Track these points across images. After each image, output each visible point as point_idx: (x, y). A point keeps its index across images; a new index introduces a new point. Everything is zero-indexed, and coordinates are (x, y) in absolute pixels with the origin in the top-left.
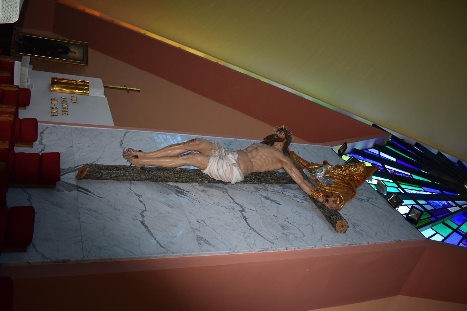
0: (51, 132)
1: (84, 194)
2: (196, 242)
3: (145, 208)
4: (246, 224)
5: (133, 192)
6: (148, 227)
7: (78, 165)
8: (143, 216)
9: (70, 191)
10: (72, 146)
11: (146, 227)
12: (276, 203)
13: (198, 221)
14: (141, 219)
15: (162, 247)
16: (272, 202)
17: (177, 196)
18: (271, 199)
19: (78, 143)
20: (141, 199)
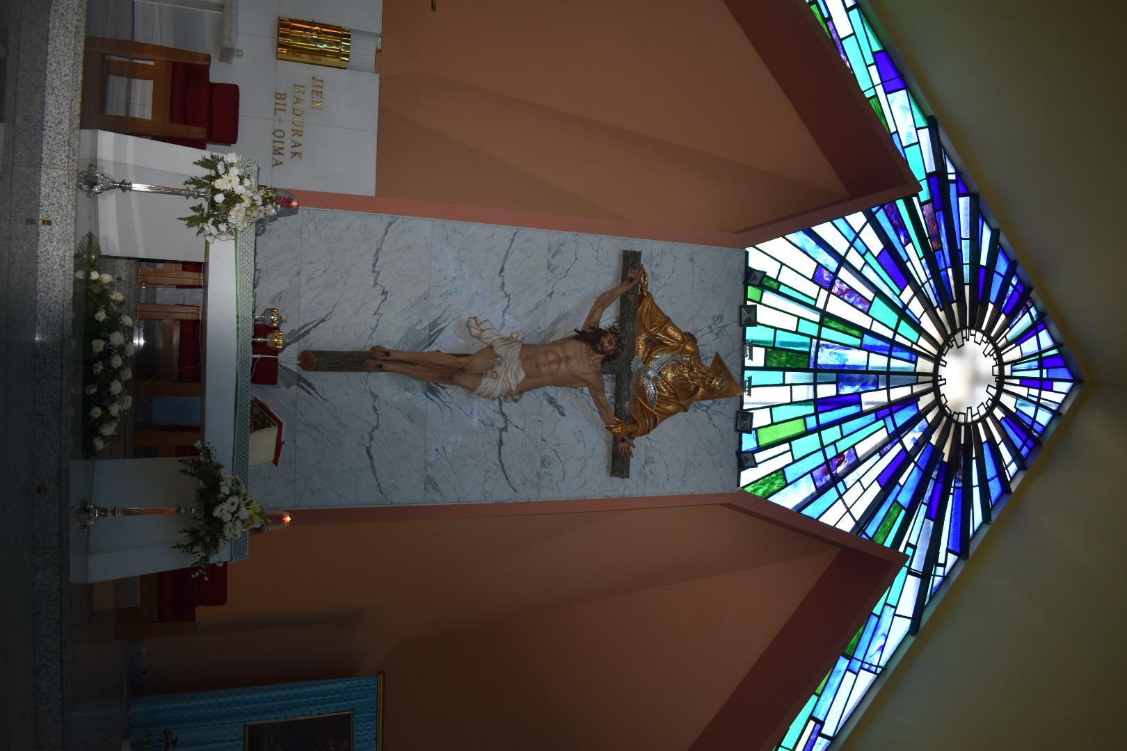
1: (307, 394)
2: (423, 486)
4: (497, 456)
5: (368, 389)
6: (373, 458)
8: (372, 438)
11: (371, 458)
12: (560, 413)
13: (437, 450)
15: (381, 492)
16: (556, 410)
17: (425, 397)
18: (556, 404)
20: (376, 404)
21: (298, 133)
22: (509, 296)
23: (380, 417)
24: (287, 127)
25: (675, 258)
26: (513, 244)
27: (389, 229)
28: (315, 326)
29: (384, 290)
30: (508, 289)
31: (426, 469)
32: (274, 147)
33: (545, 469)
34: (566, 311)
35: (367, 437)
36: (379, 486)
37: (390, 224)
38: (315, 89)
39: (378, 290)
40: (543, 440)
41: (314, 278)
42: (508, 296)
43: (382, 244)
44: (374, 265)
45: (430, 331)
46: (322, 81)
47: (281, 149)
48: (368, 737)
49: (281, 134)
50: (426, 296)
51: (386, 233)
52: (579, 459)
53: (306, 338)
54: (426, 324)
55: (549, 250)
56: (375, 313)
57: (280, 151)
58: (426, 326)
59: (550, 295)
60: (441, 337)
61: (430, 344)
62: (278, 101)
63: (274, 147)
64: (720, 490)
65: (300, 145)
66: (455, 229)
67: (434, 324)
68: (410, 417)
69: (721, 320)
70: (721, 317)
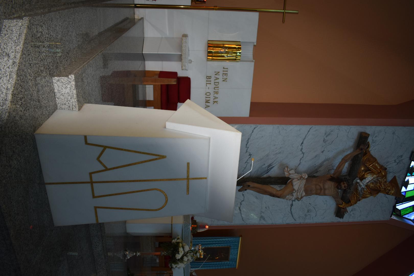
3: (244, 199)
4: (290, 209)
8: (241, 204)
11: (240, 210)
13: (266, 208)
14: (239, 206)
15: (243, 221)
21: (217, 93)
22: (304, 153)
23: (245, 198)
24: (211, 91)
25: (386, 133)
26: (309, 133)
27: (254, 131)
29: (250, 154)
30: (303, 151)
31: (261, 214)
33: (308, 213)
34: (329, 158)
35: (239, 204)
37: (255, 128)
39: (248, 154)
40: (310, 204)
42: (303, 153)
43: (251, 136)
44: (247, 145)
45: (268, 168)
46: (227, 69)
47: (209, 100)
48: (235, 253)
50: (267, 155)
51: (253, 132)
52: (323, 210)
54: (267, 165)
55: (325, 134)
56: (246, 162)
57: (209, 101)
59: (322, 152)
60: (272, 170)
61: (268, 172)
62: (208, 80)
63: (206, 100)
64: (382, 219)
65: (218, 79)
66: (283, 128)
67: (270, 165)
68: (257, 197)
69: (402, 157)
70: (402, 156)
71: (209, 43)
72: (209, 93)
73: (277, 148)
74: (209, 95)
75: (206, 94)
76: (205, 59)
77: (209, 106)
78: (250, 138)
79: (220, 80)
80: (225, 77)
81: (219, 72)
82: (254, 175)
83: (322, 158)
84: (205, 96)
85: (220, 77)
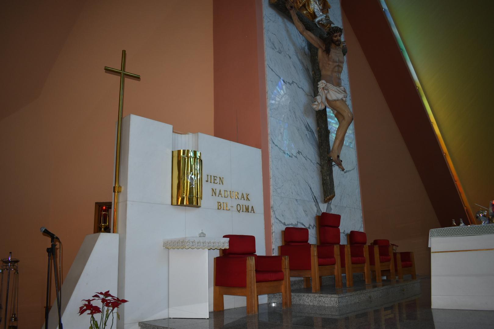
0: (282, 216)
7: (313, 199)
9: (331, 209)
10: (296, 199)
19: (292, 194)
28: (313, 193)
30: (291, 82)
32: (245, 212)
34: (294, 51)
36: (353, 169)
37: (273, 143)
38: (212, 181)
39: (298, 155)
41: (297, 191)
45: (309, 131)
46: (208, 175)
49: (239, 206)
53: (317, 199)
55: (273, 49)
56: (306, 159)
57: (247, 207)
58: (308, 132)
60: (310, 126)
61: (313, 132)
62: (222, 208)
63: (245, 212)
67: (306, 127)
71: (176, 204)
72: (237, 205)
73: (291, 116)
74: (240, 205)
75: (239, 211)
76: (196, 210)
77: (252, 207)
78: (284, 151)
79: (222, 188)
80: (218, 180)
81: (213, 190)
82: (317, 150)
83: (295, 59)
84: (241, 212)
85: (218, 187)
